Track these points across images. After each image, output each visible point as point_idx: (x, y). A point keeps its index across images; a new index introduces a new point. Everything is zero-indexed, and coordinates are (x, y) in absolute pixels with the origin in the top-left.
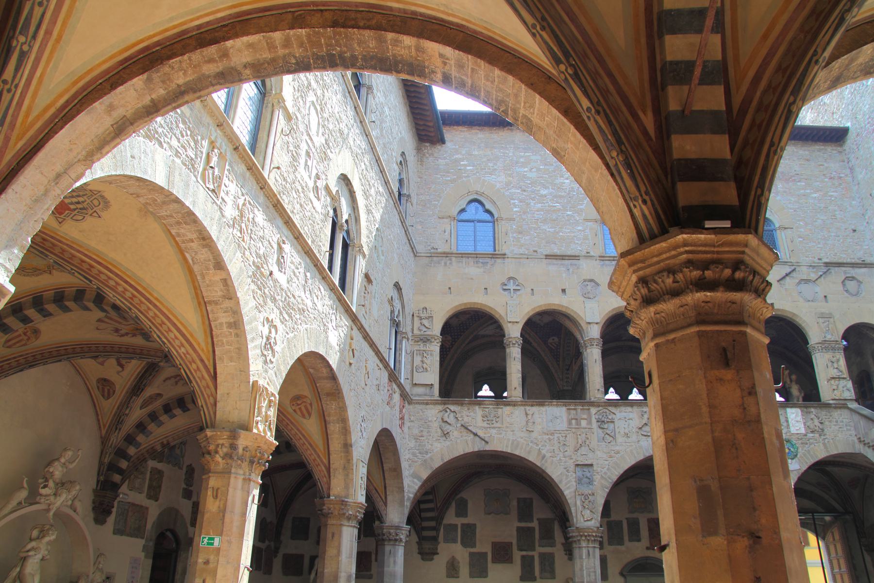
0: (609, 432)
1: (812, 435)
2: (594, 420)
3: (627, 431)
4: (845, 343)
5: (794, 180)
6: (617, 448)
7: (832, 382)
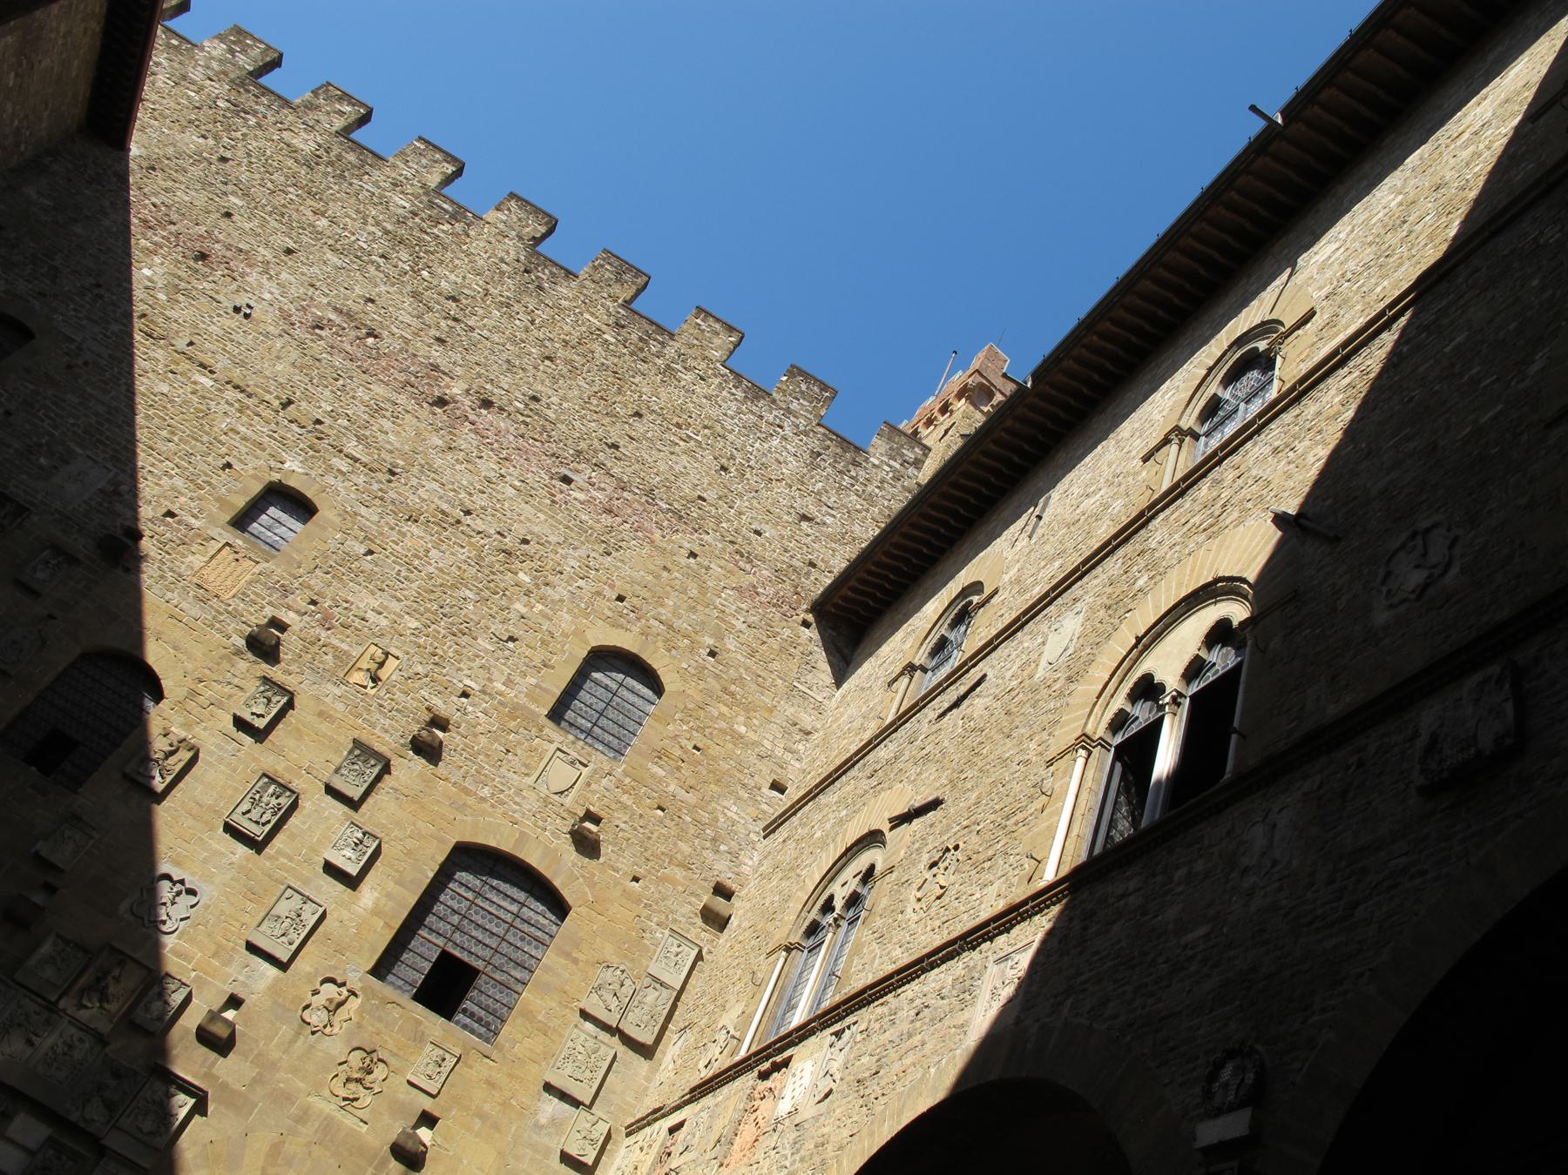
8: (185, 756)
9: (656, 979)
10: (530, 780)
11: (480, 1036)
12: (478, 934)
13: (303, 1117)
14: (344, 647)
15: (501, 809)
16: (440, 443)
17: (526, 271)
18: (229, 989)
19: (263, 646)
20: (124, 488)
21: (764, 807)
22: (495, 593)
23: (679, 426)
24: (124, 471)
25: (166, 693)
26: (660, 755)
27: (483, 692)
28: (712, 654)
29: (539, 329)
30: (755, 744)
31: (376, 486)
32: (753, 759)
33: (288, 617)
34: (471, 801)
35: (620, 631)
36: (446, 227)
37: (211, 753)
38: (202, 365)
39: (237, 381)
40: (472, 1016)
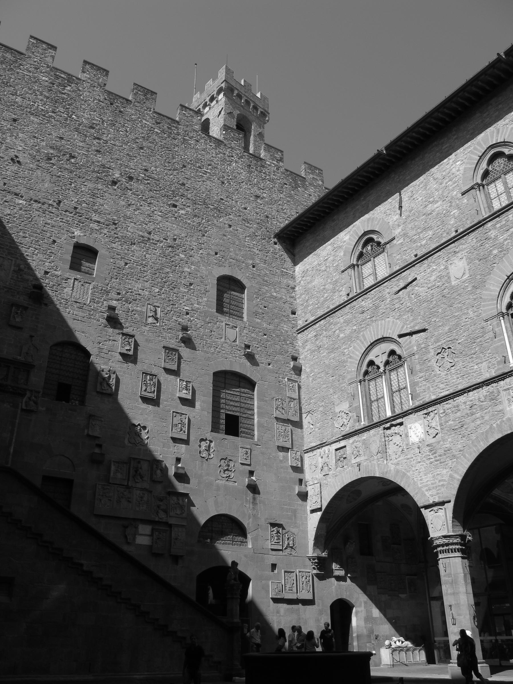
8: (113, 376)
9: (291, 398)
10: (223, 340)
11: (249, 438)
12: (231, 403)
13: (218, 488)
14: (140, 309)
15: (220, 354)
16: (124, 203)
17: (112, 104)
18: (175, 456)
19: (113, 321)
20: (22, 266)
21: (293, 322)
22: (177, 266)
23: (200, 167)
24: (17, 258)
25: (91, 353)
26: (256, 314)
27: (192, 310)
28: (254, 267)
29: (130, 134)
30: (281, 298)
31: (113, 232)
32: (283, 305)
33: (114, 303)
34: (209, 355)
35: (223, 268)
36: (69, 88)
37: (120, 371)
38: (16, 194)
39: (34, 198)
40: (244, 432)
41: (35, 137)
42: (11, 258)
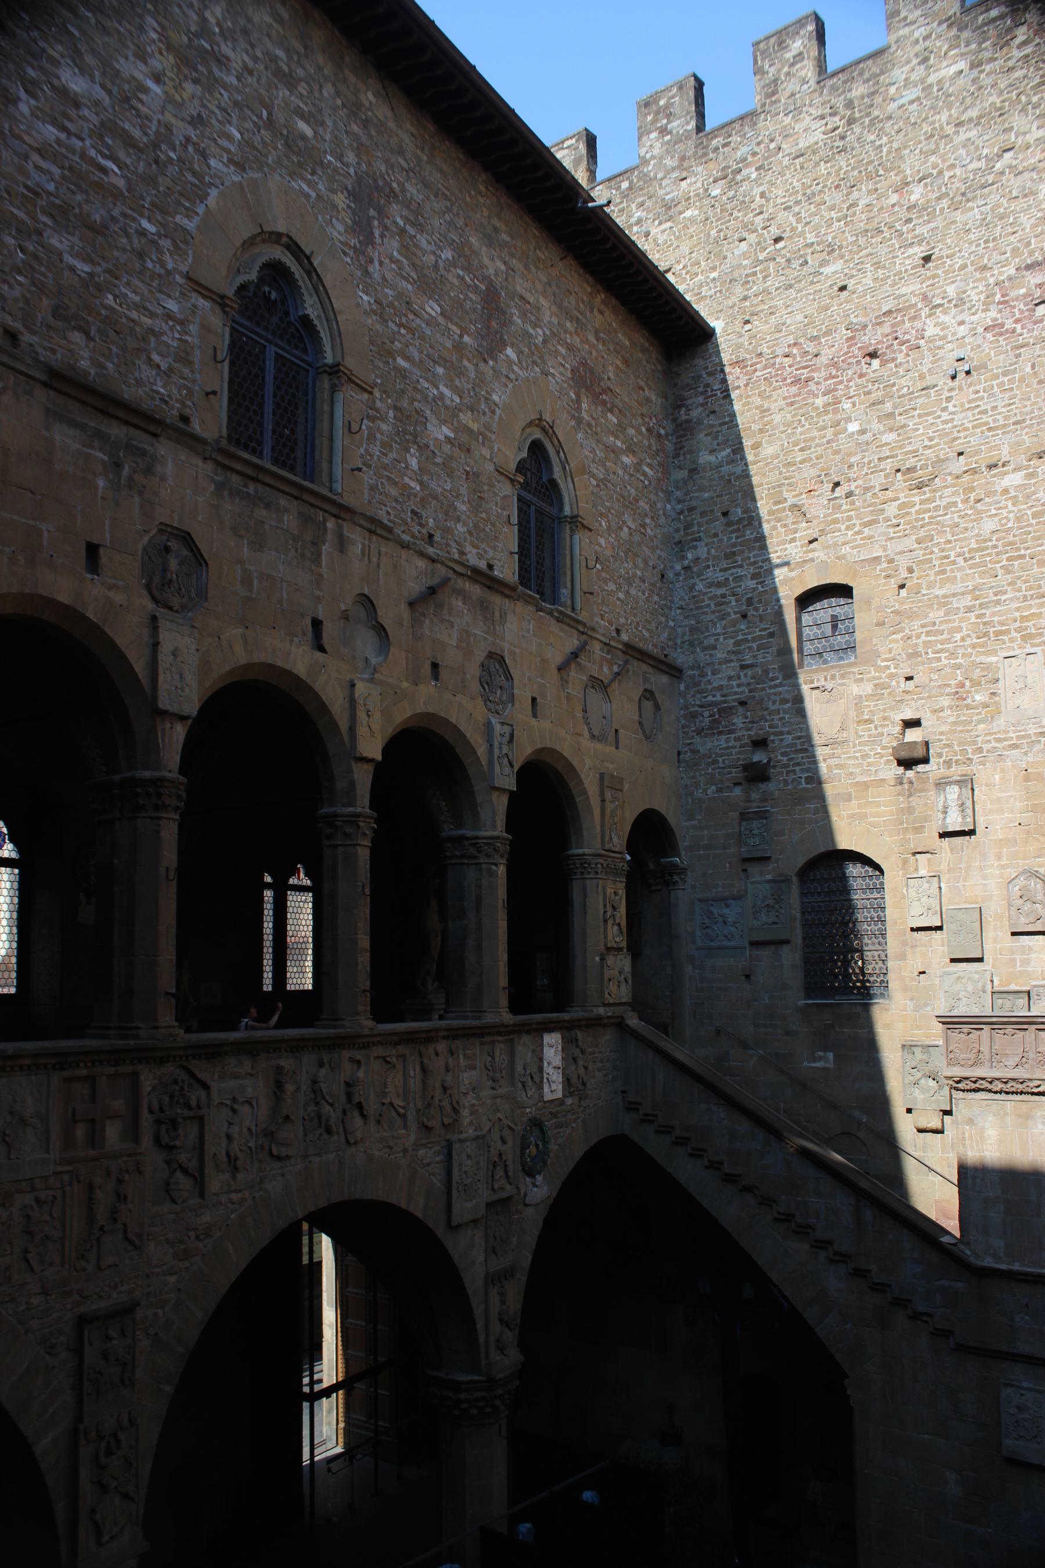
0: (183, 1157)
1: (569, 1101)
2: (146, 1119)
3: (235, 1148)
4: (628, 858)
5: (604, 403)
6: (206, 1218)
7: (610, 960)
38: (991, 467)
41: (985, 268)
42: (1033, 650)
